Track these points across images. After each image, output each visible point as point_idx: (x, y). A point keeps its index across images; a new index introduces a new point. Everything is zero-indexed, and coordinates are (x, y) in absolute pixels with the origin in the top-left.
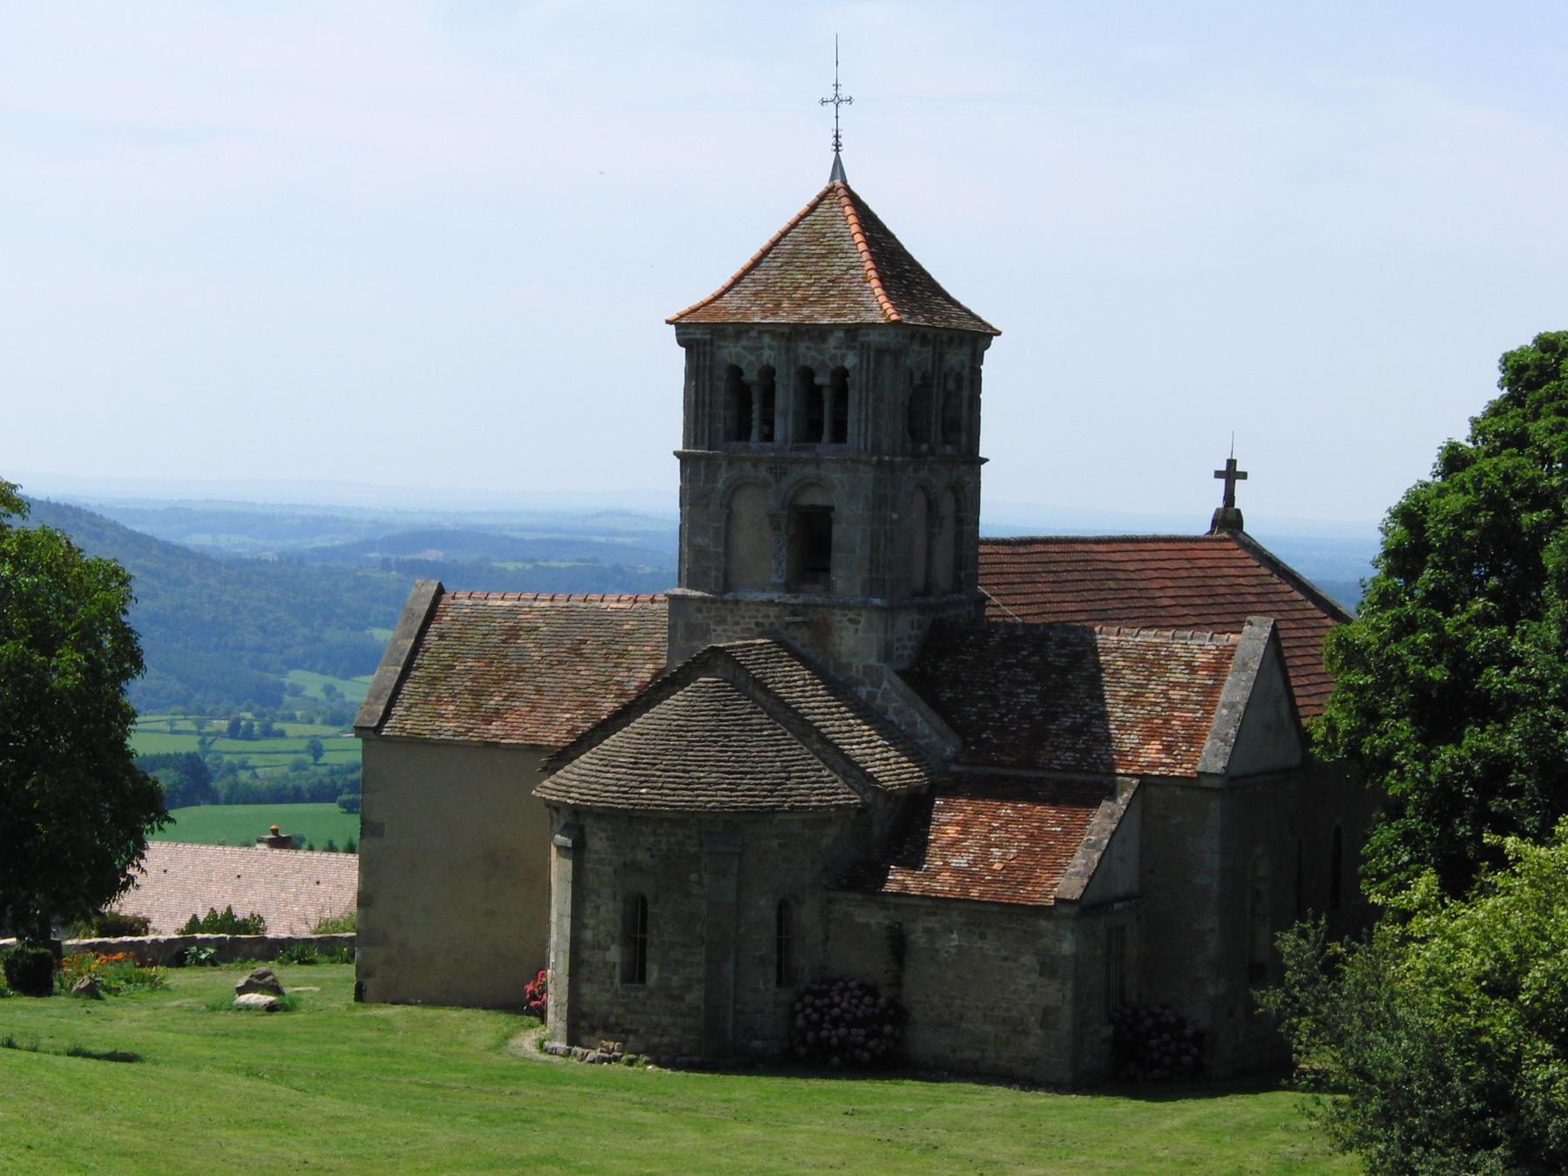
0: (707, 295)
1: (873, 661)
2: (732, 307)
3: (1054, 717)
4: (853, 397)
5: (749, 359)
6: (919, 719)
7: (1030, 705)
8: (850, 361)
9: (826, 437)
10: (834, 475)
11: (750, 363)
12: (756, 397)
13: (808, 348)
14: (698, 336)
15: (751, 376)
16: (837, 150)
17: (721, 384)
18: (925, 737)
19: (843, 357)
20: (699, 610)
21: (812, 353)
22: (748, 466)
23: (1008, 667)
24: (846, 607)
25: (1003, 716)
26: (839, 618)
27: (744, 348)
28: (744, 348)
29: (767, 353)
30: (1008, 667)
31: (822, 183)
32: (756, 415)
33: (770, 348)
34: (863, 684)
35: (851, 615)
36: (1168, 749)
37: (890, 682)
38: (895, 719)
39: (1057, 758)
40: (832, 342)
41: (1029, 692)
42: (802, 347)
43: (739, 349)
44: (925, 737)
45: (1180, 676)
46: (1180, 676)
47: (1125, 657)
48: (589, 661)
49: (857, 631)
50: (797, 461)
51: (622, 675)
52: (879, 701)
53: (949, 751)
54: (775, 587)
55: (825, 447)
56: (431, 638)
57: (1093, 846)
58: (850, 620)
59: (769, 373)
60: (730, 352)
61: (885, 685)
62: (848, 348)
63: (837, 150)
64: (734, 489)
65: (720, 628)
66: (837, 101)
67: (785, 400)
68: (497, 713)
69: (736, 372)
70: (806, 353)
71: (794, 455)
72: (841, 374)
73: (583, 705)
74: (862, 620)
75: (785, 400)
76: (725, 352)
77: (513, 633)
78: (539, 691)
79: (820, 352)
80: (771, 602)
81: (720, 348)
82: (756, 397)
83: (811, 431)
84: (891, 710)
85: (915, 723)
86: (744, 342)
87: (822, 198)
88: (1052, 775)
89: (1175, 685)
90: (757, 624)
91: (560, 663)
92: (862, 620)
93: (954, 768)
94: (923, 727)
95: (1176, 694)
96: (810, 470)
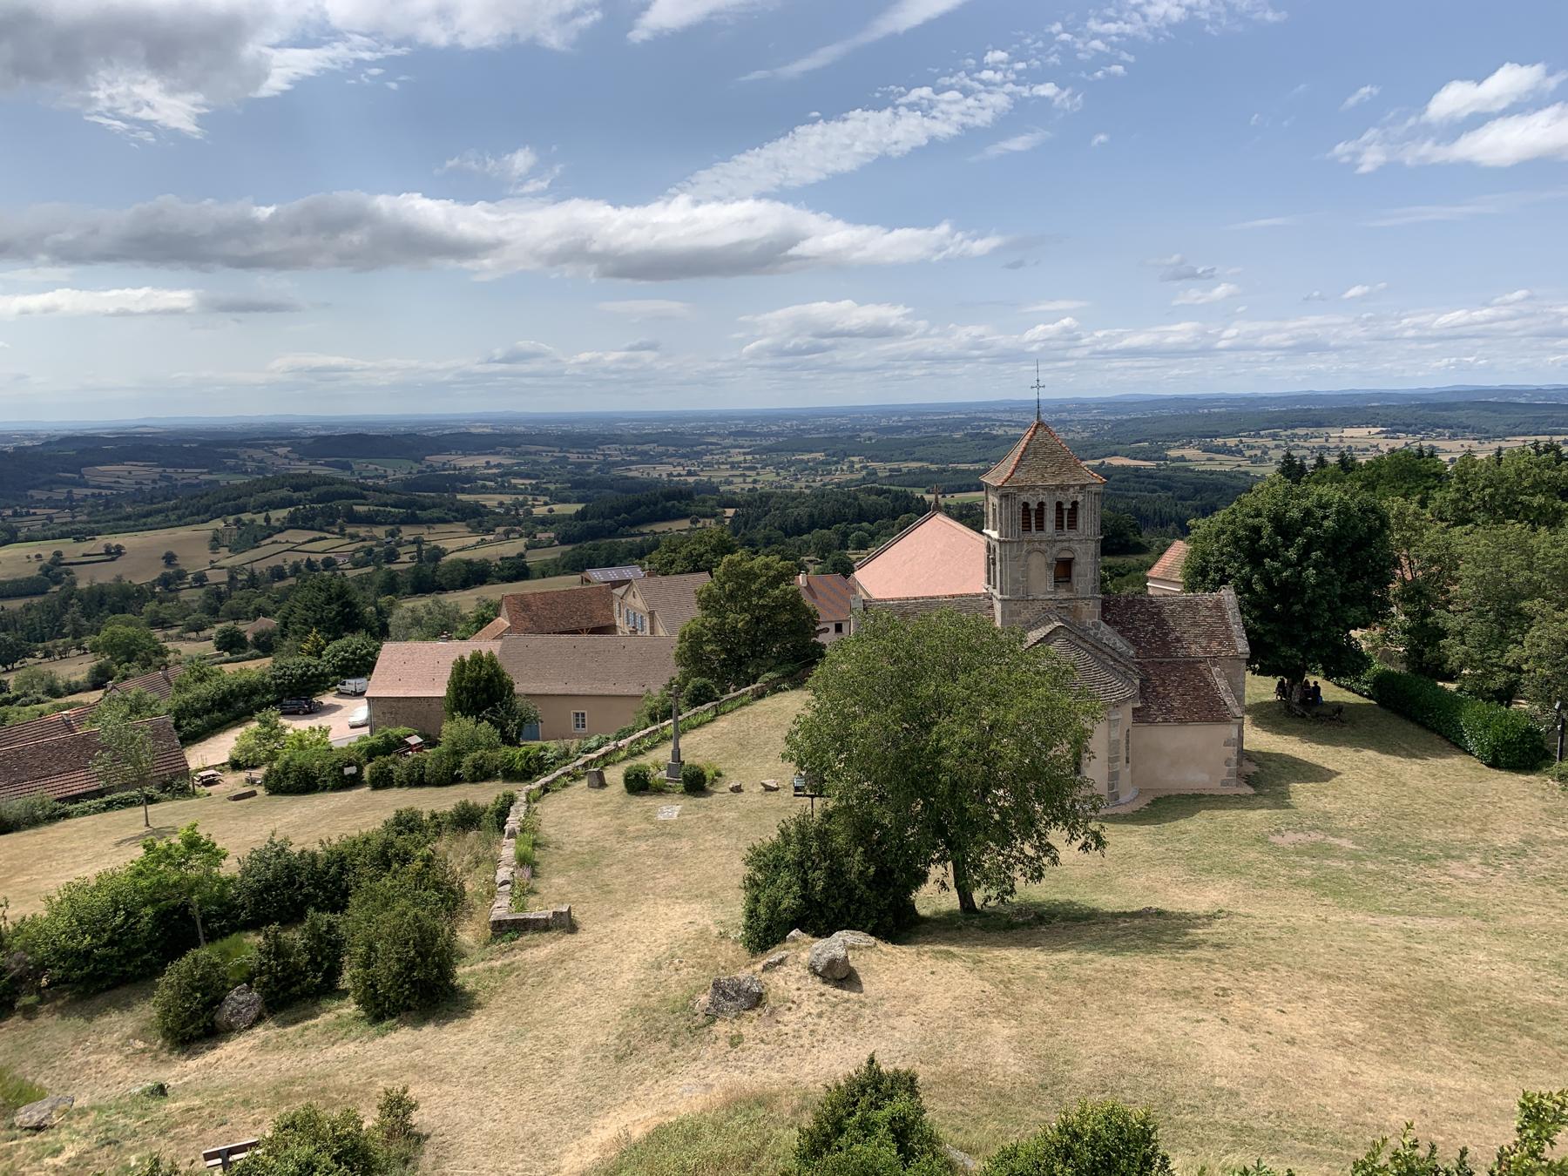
2: (1022, 477)
3: (1167, 634)
4: (1080, 513)
15: (1034, 506)
26: (1080, 603)
59: (1041, 504)
60: (1024, 497)
64: (1029, 553)
66: (1038, 387)
67: (1050, 515)
69: (1026, 505)
70: (1060, 496)
72: (1075, 504)
75: (1050, 515)
83: (1059, 525)
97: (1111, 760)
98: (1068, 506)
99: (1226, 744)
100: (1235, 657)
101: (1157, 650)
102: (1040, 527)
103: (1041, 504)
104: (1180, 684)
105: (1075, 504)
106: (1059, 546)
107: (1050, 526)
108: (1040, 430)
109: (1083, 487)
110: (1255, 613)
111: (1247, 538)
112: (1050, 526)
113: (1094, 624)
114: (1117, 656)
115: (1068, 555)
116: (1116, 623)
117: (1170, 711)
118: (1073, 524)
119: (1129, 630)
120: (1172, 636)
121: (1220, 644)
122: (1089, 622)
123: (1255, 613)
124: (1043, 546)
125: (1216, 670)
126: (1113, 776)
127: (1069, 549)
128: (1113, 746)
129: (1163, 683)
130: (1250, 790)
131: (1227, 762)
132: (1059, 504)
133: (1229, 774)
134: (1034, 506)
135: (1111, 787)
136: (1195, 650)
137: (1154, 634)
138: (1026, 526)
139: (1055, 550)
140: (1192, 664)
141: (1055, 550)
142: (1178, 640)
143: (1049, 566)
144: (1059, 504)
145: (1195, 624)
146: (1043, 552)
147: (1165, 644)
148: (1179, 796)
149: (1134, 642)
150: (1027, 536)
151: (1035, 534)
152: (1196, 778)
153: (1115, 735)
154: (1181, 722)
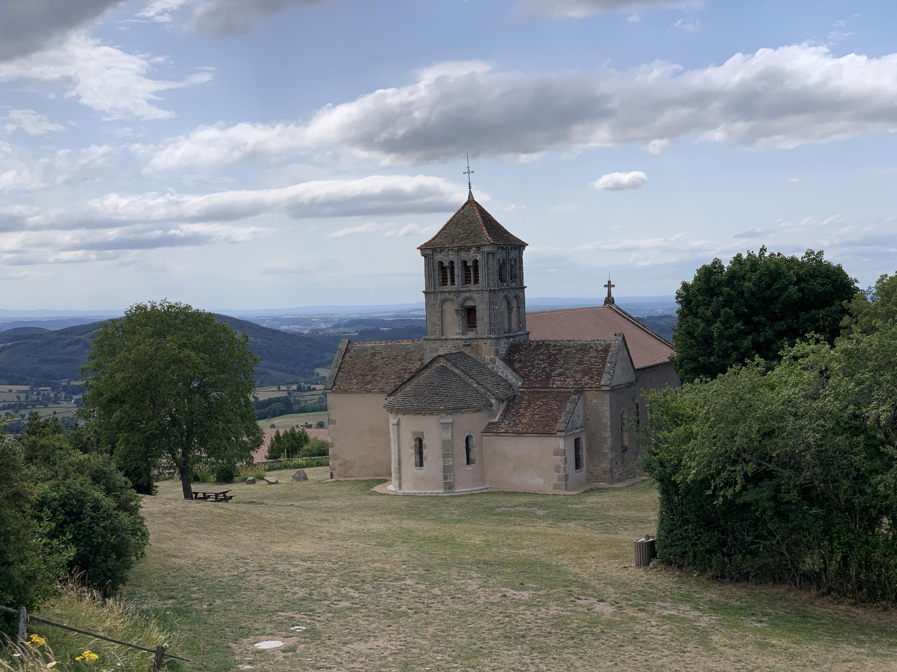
0: (430, 238)
3: (553, 370)
4: (480, 269)
5: (445, 258)
7: (545, 367)
8: (479, 257)
9: (472, 282)
10: (475, 296)
12: (448, 271)
15: (446, 264)
17: (436, 268)
26: (481, 343)
31: (466, 199)
32: (449, 277)
36: (591, 378)
40: (472, 251)
42: (462, 254)
45: (593, 354)
47: (575, 349)
53: (520, 384)
54: (458, 334)
56: (347, 358)
59: (452, 263)
60: (439, 257)
64: (443, 302)
66: (469, 172)
67: (458, 271)
68: (371, 382)
69: (441, 263)
70: (464, 255)
72: (476, 262)
73: (398, 377)
75: (458, 271)
77: (373, 355)
82: (448, 271)
83: (467, 281)
87: (466, 204)
94: (510, 377)
96: (468, 294)
99: (556, 453)
106: (463, 295)
109: (478, 247)
115: (470, 303)
122: (488, 358)
127: (470, 299)
135: (445, 478)
137: (544, 370)
139: (460, 298)
144: (465, 262)
145: (580, 363)
150: (444, 288)
151: (449, 287)
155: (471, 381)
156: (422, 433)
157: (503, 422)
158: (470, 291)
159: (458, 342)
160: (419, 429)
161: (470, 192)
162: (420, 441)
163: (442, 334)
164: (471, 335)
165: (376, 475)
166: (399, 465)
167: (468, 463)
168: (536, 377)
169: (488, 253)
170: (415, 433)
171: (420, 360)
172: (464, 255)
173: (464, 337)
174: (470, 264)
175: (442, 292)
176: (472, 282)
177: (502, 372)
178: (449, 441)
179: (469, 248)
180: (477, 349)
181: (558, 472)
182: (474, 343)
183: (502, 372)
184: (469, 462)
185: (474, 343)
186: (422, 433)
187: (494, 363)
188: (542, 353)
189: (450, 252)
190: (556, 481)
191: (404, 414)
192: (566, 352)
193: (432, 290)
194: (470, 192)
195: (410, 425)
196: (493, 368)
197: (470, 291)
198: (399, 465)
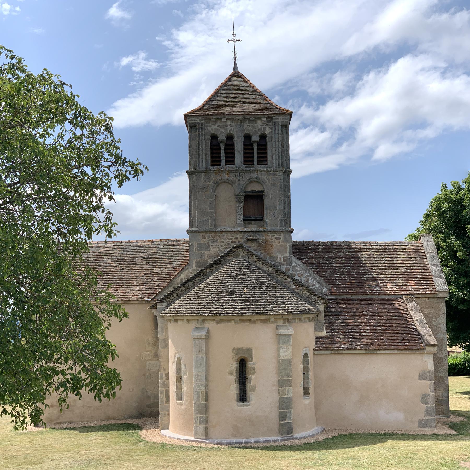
1: (288, 255)
3: (363, 275)
5: (221, 130)
6: (310, 278)
7: (349, 271)
8: (267, 131)
9: (256, 162)
10: (264, 177)
11: (221, 132)
13: (249, 126)
14: (199, 121)
15: (222, 137)
16: (235, 60)
18: (313, 285)
19: (265, 129)
20: (204, 237)
21: (250, 128)
22: (225, 174)
23: (333, 257)
24: (274, 232)
25: (340, 276)
26: (271, 237)
27: (218, 126)
28: (218, 126)
29: (229, 128)
30: (333, 257)
31: (231, 71)
33: (231, 126)
34: (283, 265)
35: (276, 236)
37: (296, 263)
38: (299, 279)
39: (374, 290)
40: (259, 122)
41: (346, 266)
42: (246, 125)
43: (216, 127)
44: (313, 285)
45: (404, 257)
46: (404, 257)
48: (141, 266)
49: (279, 242)
50: (248, 172)
51: (156, 270)
52: (291, 271)
53: (325, 290)
54: (240, 225)
55: (256, 166)
57: (421, 322)
58: (276, 238)
59: (230, 138)
60: (213, 128)
61: (294, 264)
62: (266, 125)
63: (235, 60)
64: (218, 184)
65: (214, 245)
67: (239, 147)
69: (214, 137)
70: (248, 128)
71: (248, 169)
72: (263, 137)
73: (144, 283)
74: (281, 237)
75: (239, 147)
76: (210, 129)
78: (120, 279)
79: (254, 127)
80: (239, 232)
81: (207, 127)
83: (248, 160)
84: (297, 274)
85: (308, 280)
86: (219, 123)
88: (375, 297)
89: (405, 260)
90: (232, 242)
91: (126, 267)
92: (281, 237)
93: (329, 297)
95: (407, 263)
96: (254, 175)
97: (283, 383)
98: (255, 138)
99: (422, 377)
100: (434, 296)
101: (352, 287)
102: (230, 160)
103: (230, 138)
104: (372, 317)
105: (263, 137)
106: (247, 176)
107: (239, 158)
108: (235, 78)
109: (270, 118)
110: (463, 281)
111: (451, 209)
112: (239, 158)
113: (285, 259)
114: (310, 294)
115: (255, 188)
116: (312, 264)
117: (356, 340)
118: (263, 160)
119: (325, 271)
120: (368, 276)
121: (418, 283)
122: (280, 257)
123: (463, 281)
124: (232, 177)
125: (410, 306)
126: (285, 405)
127: (257, 181)
128: (284, 367)
129: (354, 317)
130: (453, 432)
131: (424, 399)
132: (247, 137)
133: (428, 413)
134: (222, 137)
135: (282, 417)
136: (391, 288)
138: (216, 161)
139: (243, 182)
140: (388, 302)
141: (243, 182)
142: (374, 279)
143: (237, 196)
144: (247, 137)
145: (392, 266)
146: (231, 183)
147: (360, 283)
148: (365, 434)
149: (328, 281)
152: (389, 415)
153: (286, 353)
154: (368, 349)
155: (287, 280)
156: (249, 350)
157: (336, 336)
158: (257, 171)
159: (239, 236)
160: (243, 344)
161: (235, 64)
162: (243, 364)
163: (216, 226)
164: (253, 227)
165: (108, 418)
166: (207, 400)
167: (304, 394)
168: (344, 281)
169: (282, 126)
170: (237, 351)
171: (170, 263)
172: (248, 128)
173: (246, 229)
174: (255, 138)
175: (216, 172)
176: (256, 162)
177: (300, 276)
178: (290, 361)
179: (258, 117)
180: (266, 245)
181: (426, 403)
182: (261, 238)
183: (300, 276)
184: (306, 392)
185: (261, 238)
186: (249, 350)
187: (290, 264)
188: (336, 255)
189: (229, 122)
190: (422, 416)
191: (218, 322)
192: (368, 255)
193: (203, 168)
194: (235, 64)
195: (229, 338)
196: (288, 270)
197: (257, 171)
198: (207, 400)
